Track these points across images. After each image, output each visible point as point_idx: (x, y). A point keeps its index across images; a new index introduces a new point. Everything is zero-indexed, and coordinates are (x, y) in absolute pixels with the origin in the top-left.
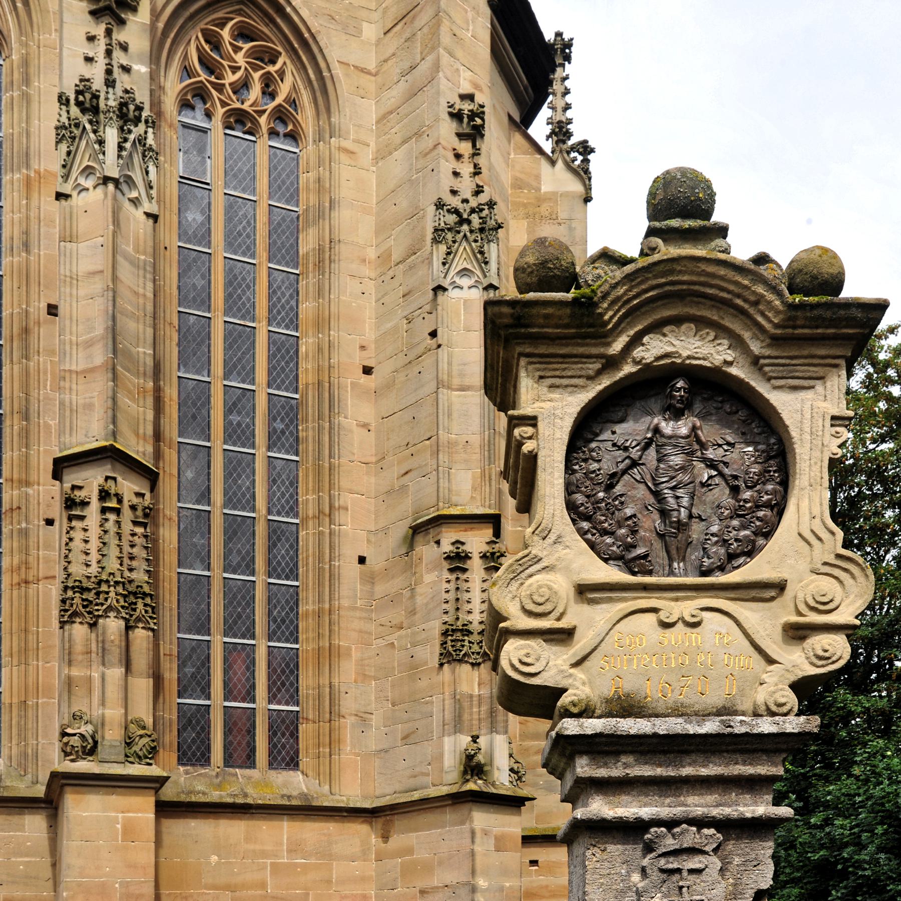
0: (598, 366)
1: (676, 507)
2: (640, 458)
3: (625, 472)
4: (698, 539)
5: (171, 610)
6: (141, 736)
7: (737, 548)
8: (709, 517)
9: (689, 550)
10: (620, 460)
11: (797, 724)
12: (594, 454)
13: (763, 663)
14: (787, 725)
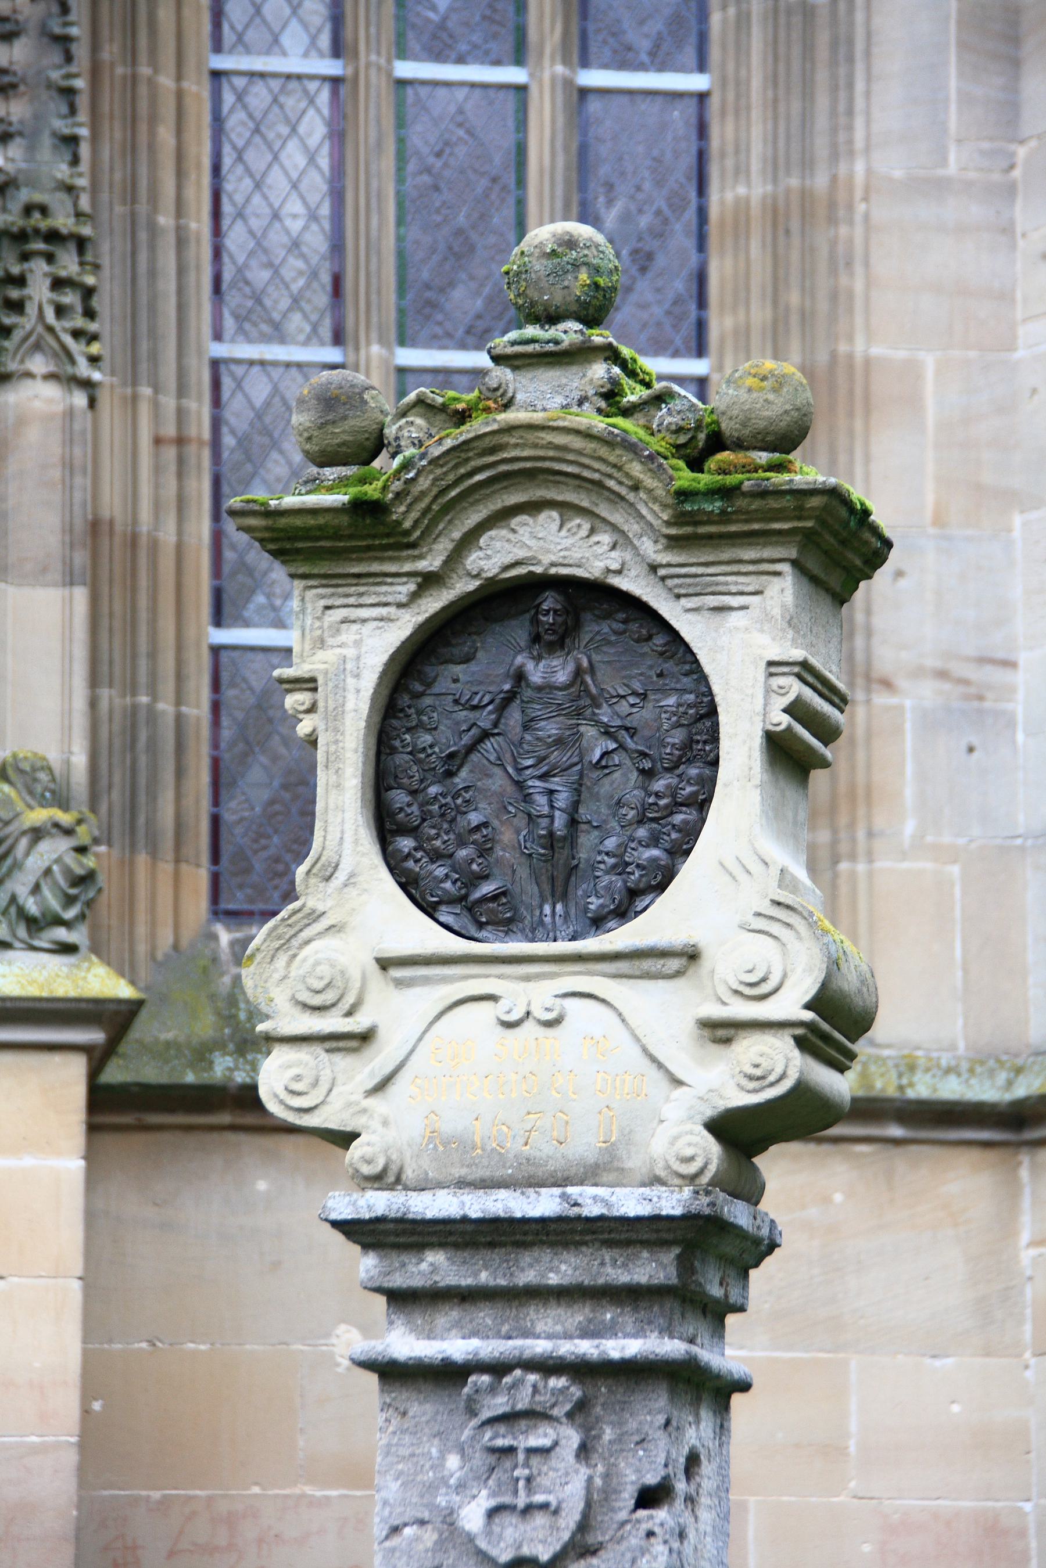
0: (412, 587)
1: (546, 810)
2: (496, 725)
3: (471, 749)
4: (587, 860)
6: (37, 834)
7: (639, 880)
8: (605, 821)
9: (573, 879)
10: (464, 728)
11: (679, 1201)
12: (425, 718)
13: (664, 1083)
14: (663, 1203)
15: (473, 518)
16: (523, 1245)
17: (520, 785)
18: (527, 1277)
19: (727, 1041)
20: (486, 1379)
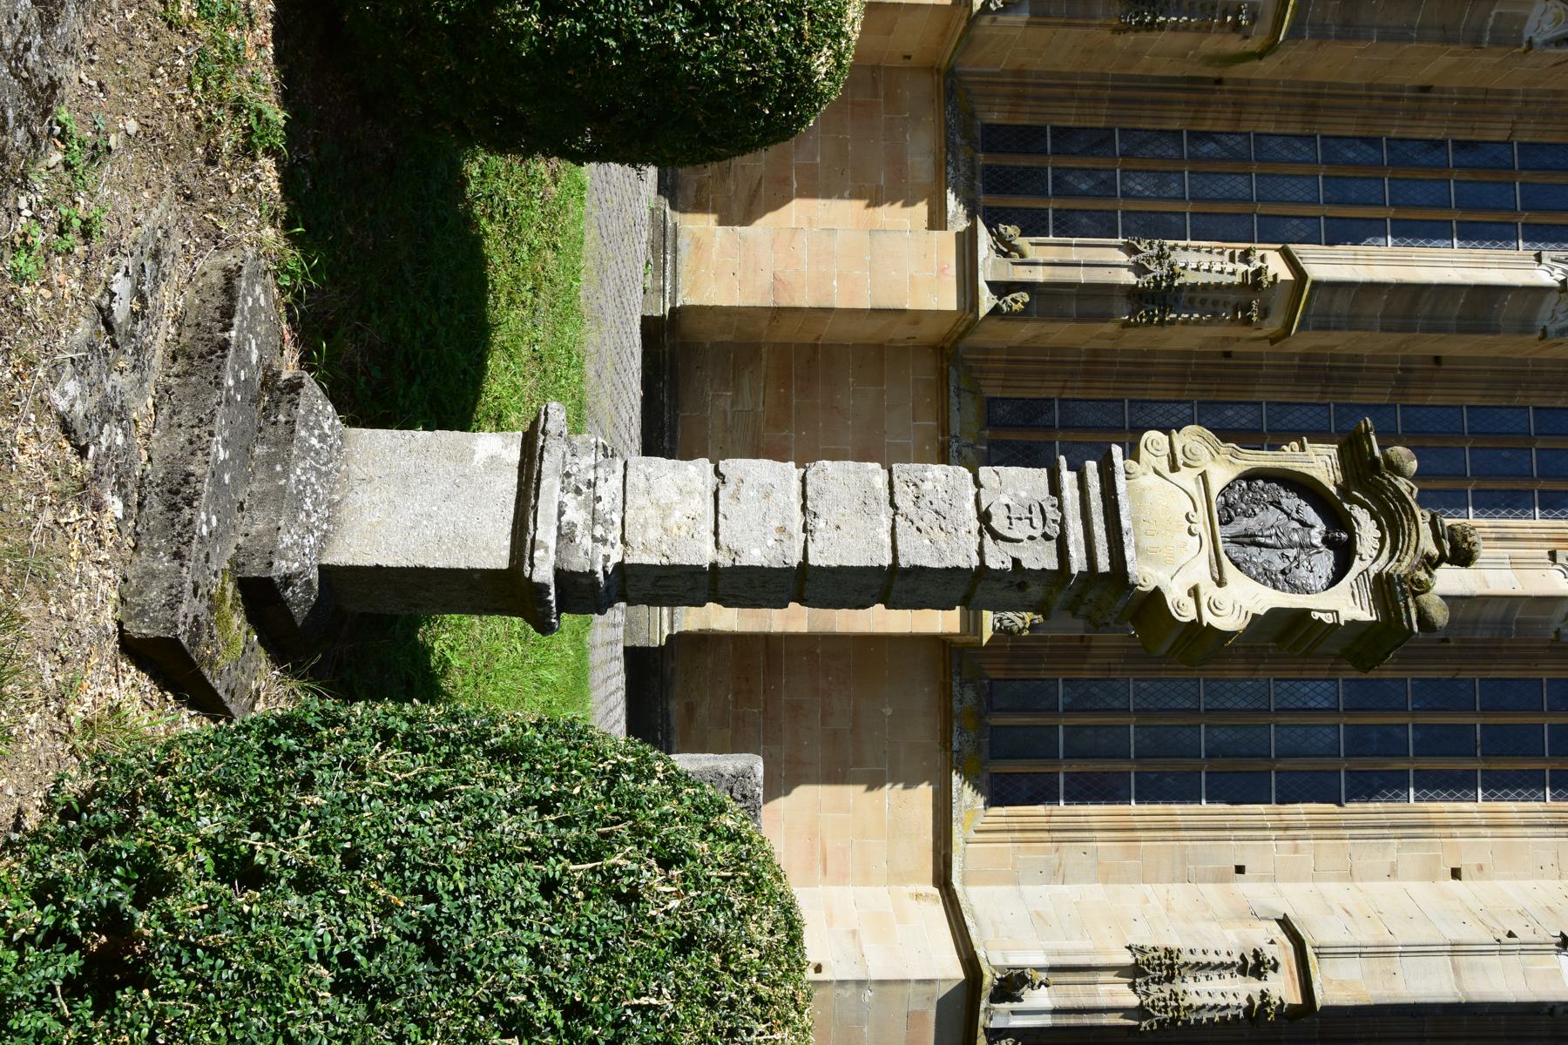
5: (1158, 670)
19: (1189, 595)
20: (1056, 502)
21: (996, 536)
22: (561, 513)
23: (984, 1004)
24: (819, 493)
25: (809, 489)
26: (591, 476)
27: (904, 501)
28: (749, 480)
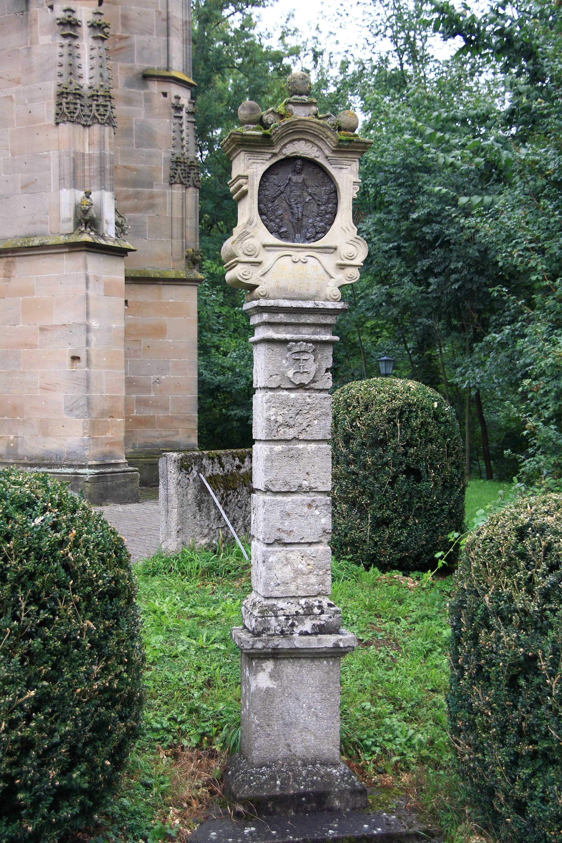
15: (286, 141)
16: (302, 314)
17: (290, 206)
18: (303, 321)
19: (343, 269)
21: (313, 381)
22: (306, 634)
23: (103, 242)
24: (286, 483)
25: (283, 490)
26: (282, 618)
27: (291, 433)
28: (279, 525)
